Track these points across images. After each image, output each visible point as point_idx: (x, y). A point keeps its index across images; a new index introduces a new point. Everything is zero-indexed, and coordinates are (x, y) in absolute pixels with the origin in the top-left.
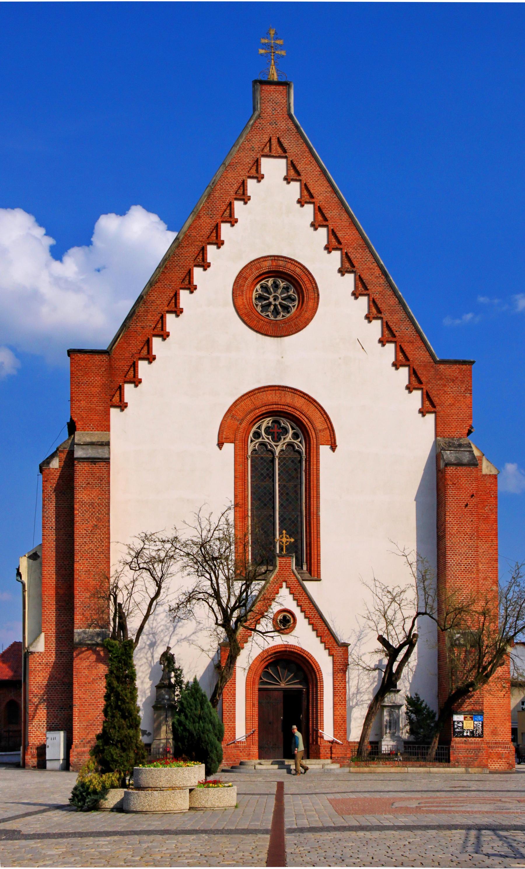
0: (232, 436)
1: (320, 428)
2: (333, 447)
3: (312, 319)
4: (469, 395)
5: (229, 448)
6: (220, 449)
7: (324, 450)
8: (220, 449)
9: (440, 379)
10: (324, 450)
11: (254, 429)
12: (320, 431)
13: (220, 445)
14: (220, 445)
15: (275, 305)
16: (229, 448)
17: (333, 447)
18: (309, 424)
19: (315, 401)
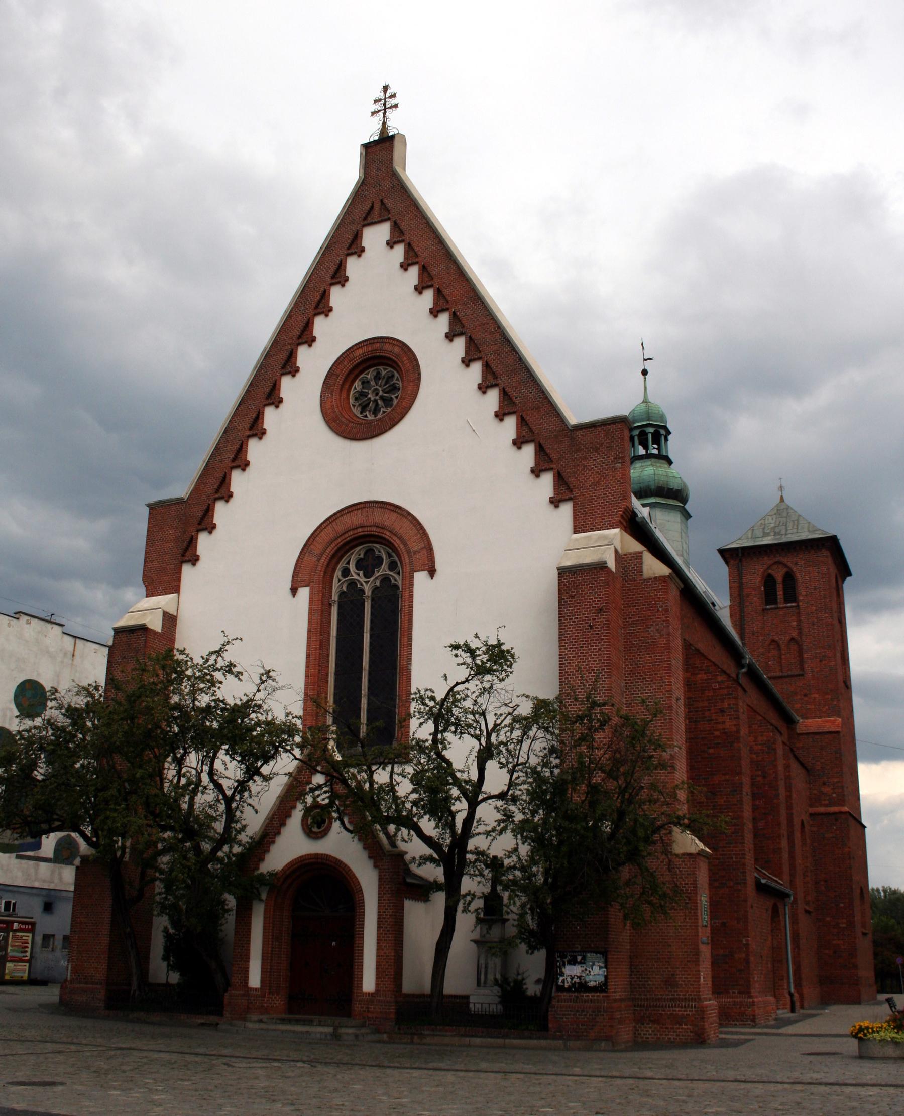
0: (307, 578)
1: (416, 549)
2: (432, 572)
3: (410, 407)
4: (620, 465)
5: (304, 593)
6: (294, 596)
7: (420, 578)
8: (294, 596)
9: (578, 450)
10: (420, 578)
11: (342, 564)
12: (415, 553)
13: (294, 591)
14: (294, 591)
15: (382, 398)
16: (304, 593)
17: (432, 572)
18: (402, 546)
19: (409, 513)
